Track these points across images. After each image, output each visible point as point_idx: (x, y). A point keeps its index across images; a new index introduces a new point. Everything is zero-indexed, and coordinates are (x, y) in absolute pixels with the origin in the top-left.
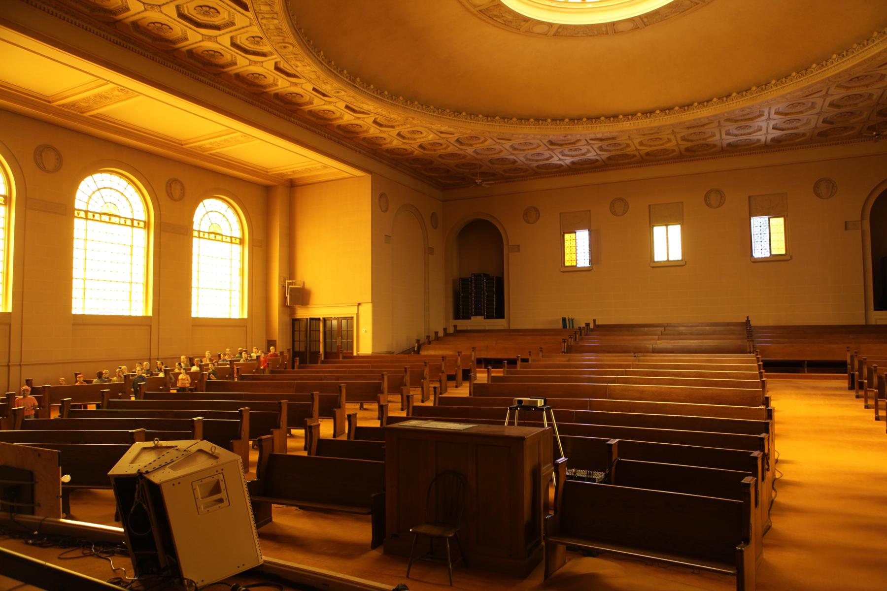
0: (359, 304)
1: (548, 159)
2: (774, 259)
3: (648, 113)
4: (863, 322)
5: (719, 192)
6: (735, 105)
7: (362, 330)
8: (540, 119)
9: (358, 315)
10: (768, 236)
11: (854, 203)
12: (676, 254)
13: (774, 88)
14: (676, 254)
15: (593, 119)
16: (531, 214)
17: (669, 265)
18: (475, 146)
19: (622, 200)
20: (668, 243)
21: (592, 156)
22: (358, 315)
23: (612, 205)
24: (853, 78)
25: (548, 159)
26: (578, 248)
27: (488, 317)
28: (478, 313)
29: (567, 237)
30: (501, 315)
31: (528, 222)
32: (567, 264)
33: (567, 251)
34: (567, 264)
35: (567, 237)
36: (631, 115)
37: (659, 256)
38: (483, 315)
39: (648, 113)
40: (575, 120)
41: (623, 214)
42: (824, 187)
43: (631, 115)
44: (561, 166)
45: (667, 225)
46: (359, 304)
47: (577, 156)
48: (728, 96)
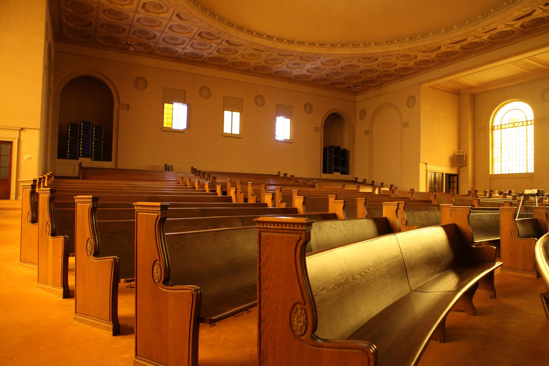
0: (22, 129)
1: (175, 45)
2: (286, 142)
3: (270, 38)
4: (319, 178)
5: (262, 97)
6: (317, 50)
7: (25, 157)
8: (213, 14)
9: (19, 140)
10: (283, 129)
11: (318, 119)
12: (236, 131)
13: (339, 49)
14: (236, 131)
15: (240, 28)
16: (141, 83)
17: (231, 136)
18: (150, 14)
19: (208, 88)
20: (232, 122)
21: (205, 53)
22: (19, 140)
23: (201, 91)
24: (367, 58)
25: (175, 45)
26: (176, 116)
27: (96, 159)
28: (85, 155)
29: (166, 105)
30: (108, 158)
31: (137, 88)
32: (165, 125)
33: (165, 116)
34: (165, 125)
35: (166, 105)
36: (260, 35)
37: (227, 130)
38: (91, 157)
39: (270, 38)
40: (230, 24)
41: (209, 97)
42: (308, 108)
43: (260, 35)
44: (177, 51)
45: (232, 111)
46: (22, 129)
47: (197, 49)
48: (314, 44)
